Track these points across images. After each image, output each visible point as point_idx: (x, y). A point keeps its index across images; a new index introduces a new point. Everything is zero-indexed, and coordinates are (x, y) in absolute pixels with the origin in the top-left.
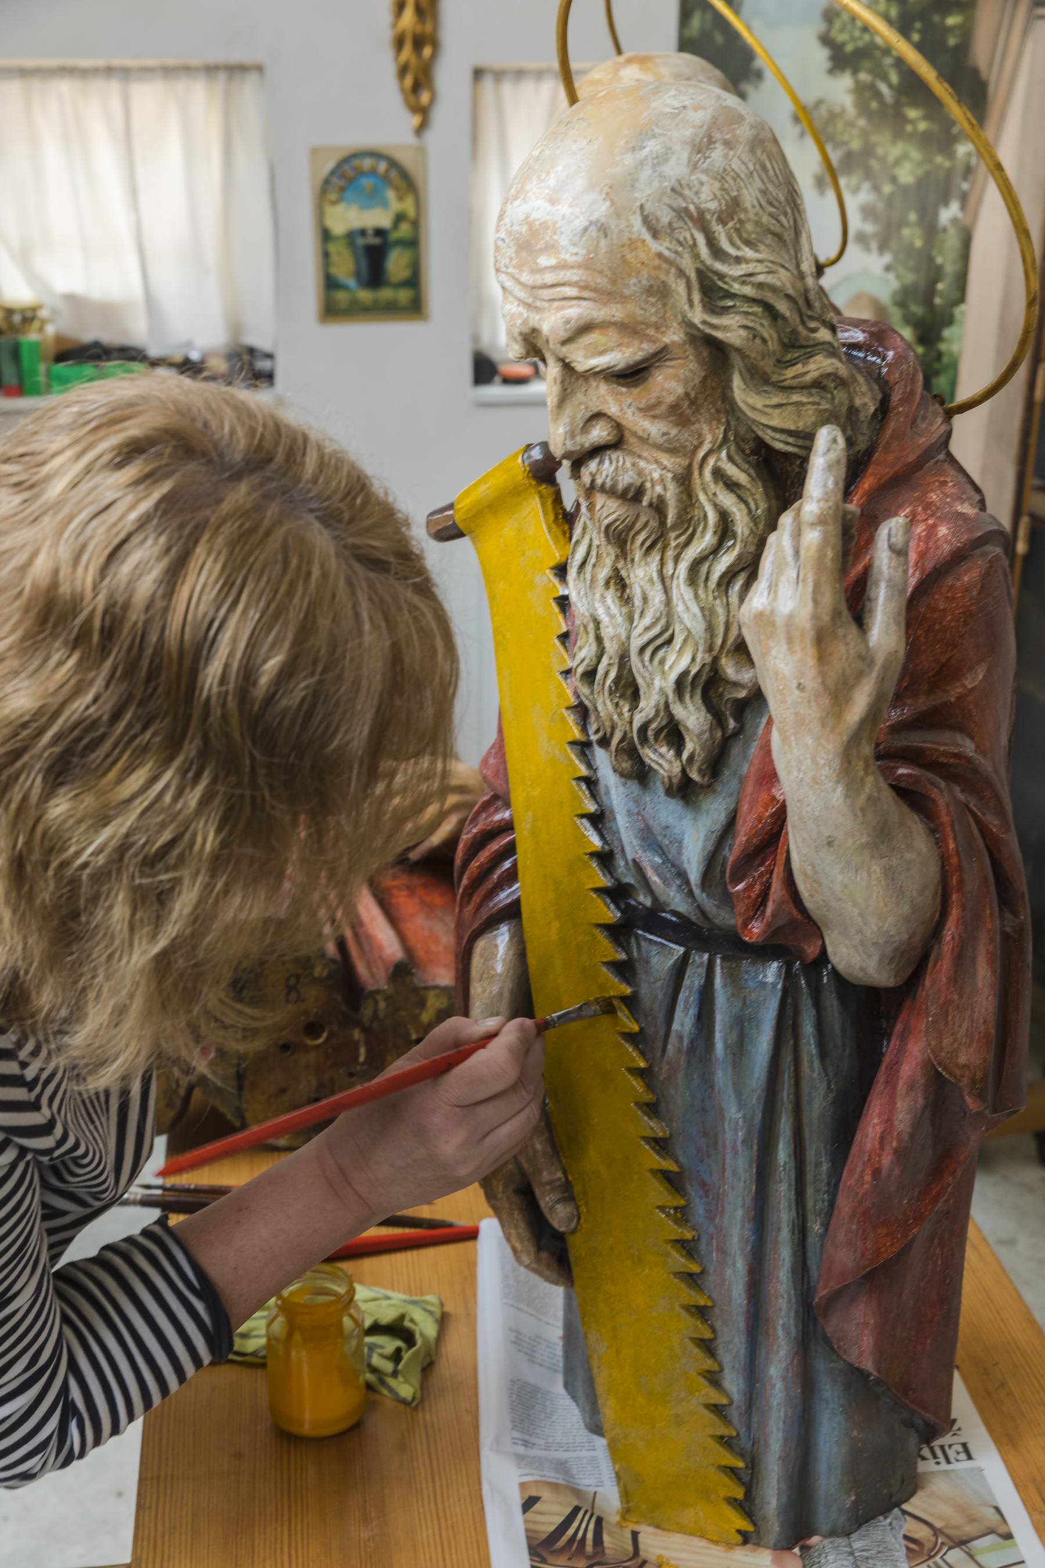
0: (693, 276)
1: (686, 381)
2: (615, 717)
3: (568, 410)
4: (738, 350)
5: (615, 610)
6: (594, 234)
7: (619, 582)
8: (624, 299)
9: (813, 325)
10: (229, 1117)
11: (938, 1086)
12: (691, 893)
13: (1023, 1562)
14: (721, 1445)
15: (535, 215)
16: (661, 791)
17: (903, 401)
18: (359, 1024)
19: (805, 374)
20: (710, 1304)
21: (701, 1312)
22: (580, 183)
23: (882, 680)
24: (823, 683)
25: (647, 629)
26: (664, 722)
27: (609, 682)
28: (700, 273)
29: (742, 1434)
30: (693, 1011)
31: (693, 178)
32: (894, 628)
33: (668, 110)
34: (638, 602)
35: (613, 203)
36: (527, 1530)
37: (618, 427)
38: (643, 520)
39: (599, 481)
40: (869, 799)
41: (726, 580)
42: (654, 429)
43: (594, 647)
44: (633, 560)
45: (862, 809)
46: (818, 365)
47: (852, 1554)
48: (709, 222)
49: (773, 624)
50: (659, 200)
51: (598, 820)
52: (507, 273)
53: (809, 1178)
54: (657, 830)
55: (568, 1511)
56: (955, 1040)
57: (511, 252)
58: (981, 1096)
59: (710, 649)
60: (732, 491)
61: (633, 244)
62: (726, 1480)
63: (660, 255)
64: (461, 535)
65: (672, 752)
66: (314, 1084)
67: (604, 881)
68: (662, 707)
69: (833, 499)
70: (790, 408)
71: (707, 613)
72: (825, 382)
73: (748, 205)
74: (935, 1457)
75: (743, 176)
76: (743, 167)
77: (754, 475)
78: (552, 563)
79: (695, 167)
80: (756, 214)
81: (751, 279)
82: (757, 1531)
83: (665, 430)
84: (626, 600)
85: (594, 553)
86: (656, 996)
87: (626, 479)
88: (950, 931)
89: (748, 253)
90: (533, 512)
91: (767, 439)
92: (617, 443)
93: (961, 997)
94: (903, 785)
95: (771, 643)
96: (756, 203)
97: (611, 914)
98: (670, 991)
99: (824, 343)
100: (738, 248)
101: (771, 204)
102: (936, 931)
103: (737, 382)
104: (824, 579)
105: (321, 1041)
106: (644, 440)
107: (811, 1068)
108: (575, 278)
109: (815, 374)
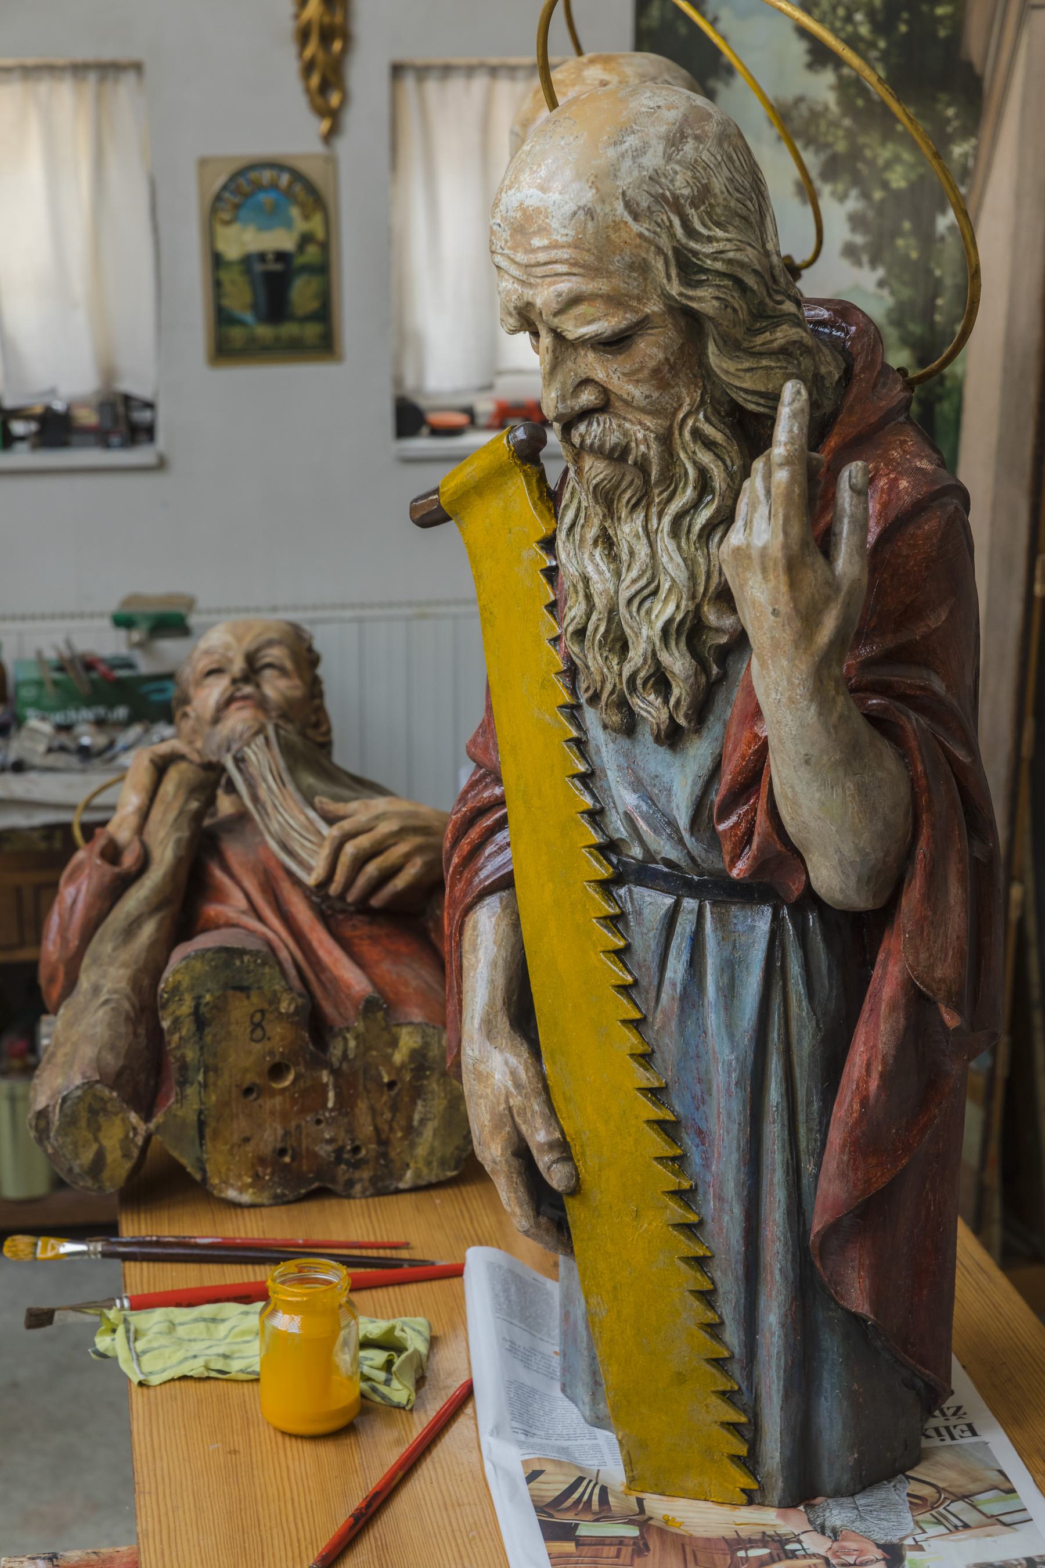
0: (670, 253)
1: (666, 348)
2: (605, 670)
3: (560, 377)
4: (710, 319)
5: (603, 567)
6: (582, 218)
7: (607, 541)
8: (609, 274)
9: (778, 298)
10: (189, 1169)
11: (917, 1001)
12: (681, 841)
13: (1025, 1510)
14: (724, 1401)
15: (528, 202)
16: (649, 739)
17: (863, 370)
18: (327, 1065)
19: (772, 341)
20: (709, 1254)
21: (700, 1263)
22: (568, 173)
23: (847, 605)
24: (796, 608)
25: (634, 581)
26: (652, 671)
27: (598, 637)
28: (676, 251)
29: (744, 1387)
30: (685, 957)
31: (668, 168)
32: (857, 558)
33: (644, 109)
34: (625, 556)
35: (598, 190)
36: (531, 1496)
37: (605, 392)
38: (628, 478)
39: (588, 442)
40: (840, 717)
41: (706, 532)
42: (636, 392)
43: (583, 605)
44: (619, 518)
45: (835, 727)
46: (784, 334)
47: (857, 1509)
48: (684, 206)
49: (749, 557)
50: (639, 188)
51: (587, 779)
52: (502, 254)
53: (802, 1117)
54: (647, 780)
55: (572, 1480)
56: (931, 955)
57: (506, 235)
58: (957, 1008)
59: (693, 597)
60: (710, 449)
61: (617, 226)
62: (729, 1436)
63: (641, 235)
64: (447, 519)
65: (659, 700)
66: (280, 1132)
67: (596, 838)
68: (649, 654)
69: (798, 442)
70: (760, 372)
71: (689, 563)
72: (791, 349)
73: (717, 191)
74: (939, 1434)
75: (712, 166)
76: (712, 159)
77: (730, 434)
78: (538, 537)
79: (669, 159)
80: (725, 199)
81: (722, 256)
82: (762, 1489)
83: (648, 393)
84: (613, 557)
85: (582, 515)
86: (650, 946)
87: (613, 439)
88: (922, 850)
89: (719, 233)
90: (518, 490)
91: (740, 401)
92: (605, 406)
93: (935, 913)
94: (874, 713)
95: (748, 575)
96: (724, 189)
98: (663, 940)
99: (790, 314)
100: (710, 229)
101: (738, 190)
102: (908, 855)
103: (711, 348)
104: (792, 513)
105: (287, 1083)
106: (627, 403)
107: (800, 1006)
108: (566, 256)
109: (781, 342)
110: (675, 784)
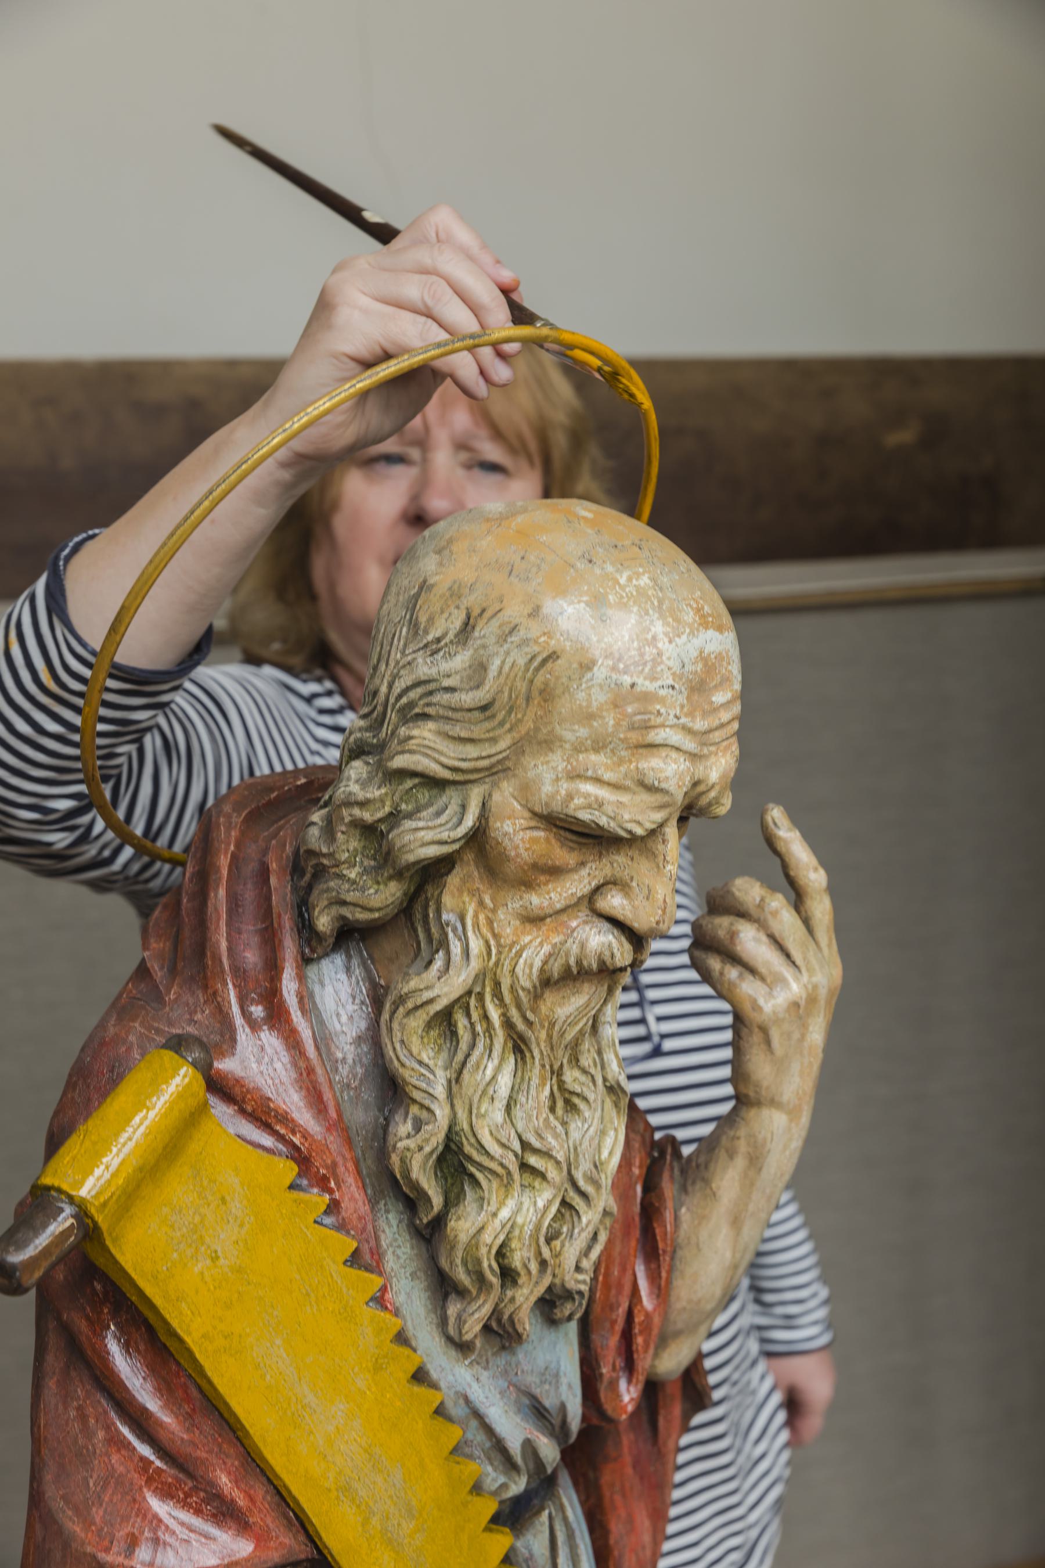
52: (671, 727)
57: (682, 699)
67: (490, 1507)
97: (502, 1541)
110: (562, 1364)
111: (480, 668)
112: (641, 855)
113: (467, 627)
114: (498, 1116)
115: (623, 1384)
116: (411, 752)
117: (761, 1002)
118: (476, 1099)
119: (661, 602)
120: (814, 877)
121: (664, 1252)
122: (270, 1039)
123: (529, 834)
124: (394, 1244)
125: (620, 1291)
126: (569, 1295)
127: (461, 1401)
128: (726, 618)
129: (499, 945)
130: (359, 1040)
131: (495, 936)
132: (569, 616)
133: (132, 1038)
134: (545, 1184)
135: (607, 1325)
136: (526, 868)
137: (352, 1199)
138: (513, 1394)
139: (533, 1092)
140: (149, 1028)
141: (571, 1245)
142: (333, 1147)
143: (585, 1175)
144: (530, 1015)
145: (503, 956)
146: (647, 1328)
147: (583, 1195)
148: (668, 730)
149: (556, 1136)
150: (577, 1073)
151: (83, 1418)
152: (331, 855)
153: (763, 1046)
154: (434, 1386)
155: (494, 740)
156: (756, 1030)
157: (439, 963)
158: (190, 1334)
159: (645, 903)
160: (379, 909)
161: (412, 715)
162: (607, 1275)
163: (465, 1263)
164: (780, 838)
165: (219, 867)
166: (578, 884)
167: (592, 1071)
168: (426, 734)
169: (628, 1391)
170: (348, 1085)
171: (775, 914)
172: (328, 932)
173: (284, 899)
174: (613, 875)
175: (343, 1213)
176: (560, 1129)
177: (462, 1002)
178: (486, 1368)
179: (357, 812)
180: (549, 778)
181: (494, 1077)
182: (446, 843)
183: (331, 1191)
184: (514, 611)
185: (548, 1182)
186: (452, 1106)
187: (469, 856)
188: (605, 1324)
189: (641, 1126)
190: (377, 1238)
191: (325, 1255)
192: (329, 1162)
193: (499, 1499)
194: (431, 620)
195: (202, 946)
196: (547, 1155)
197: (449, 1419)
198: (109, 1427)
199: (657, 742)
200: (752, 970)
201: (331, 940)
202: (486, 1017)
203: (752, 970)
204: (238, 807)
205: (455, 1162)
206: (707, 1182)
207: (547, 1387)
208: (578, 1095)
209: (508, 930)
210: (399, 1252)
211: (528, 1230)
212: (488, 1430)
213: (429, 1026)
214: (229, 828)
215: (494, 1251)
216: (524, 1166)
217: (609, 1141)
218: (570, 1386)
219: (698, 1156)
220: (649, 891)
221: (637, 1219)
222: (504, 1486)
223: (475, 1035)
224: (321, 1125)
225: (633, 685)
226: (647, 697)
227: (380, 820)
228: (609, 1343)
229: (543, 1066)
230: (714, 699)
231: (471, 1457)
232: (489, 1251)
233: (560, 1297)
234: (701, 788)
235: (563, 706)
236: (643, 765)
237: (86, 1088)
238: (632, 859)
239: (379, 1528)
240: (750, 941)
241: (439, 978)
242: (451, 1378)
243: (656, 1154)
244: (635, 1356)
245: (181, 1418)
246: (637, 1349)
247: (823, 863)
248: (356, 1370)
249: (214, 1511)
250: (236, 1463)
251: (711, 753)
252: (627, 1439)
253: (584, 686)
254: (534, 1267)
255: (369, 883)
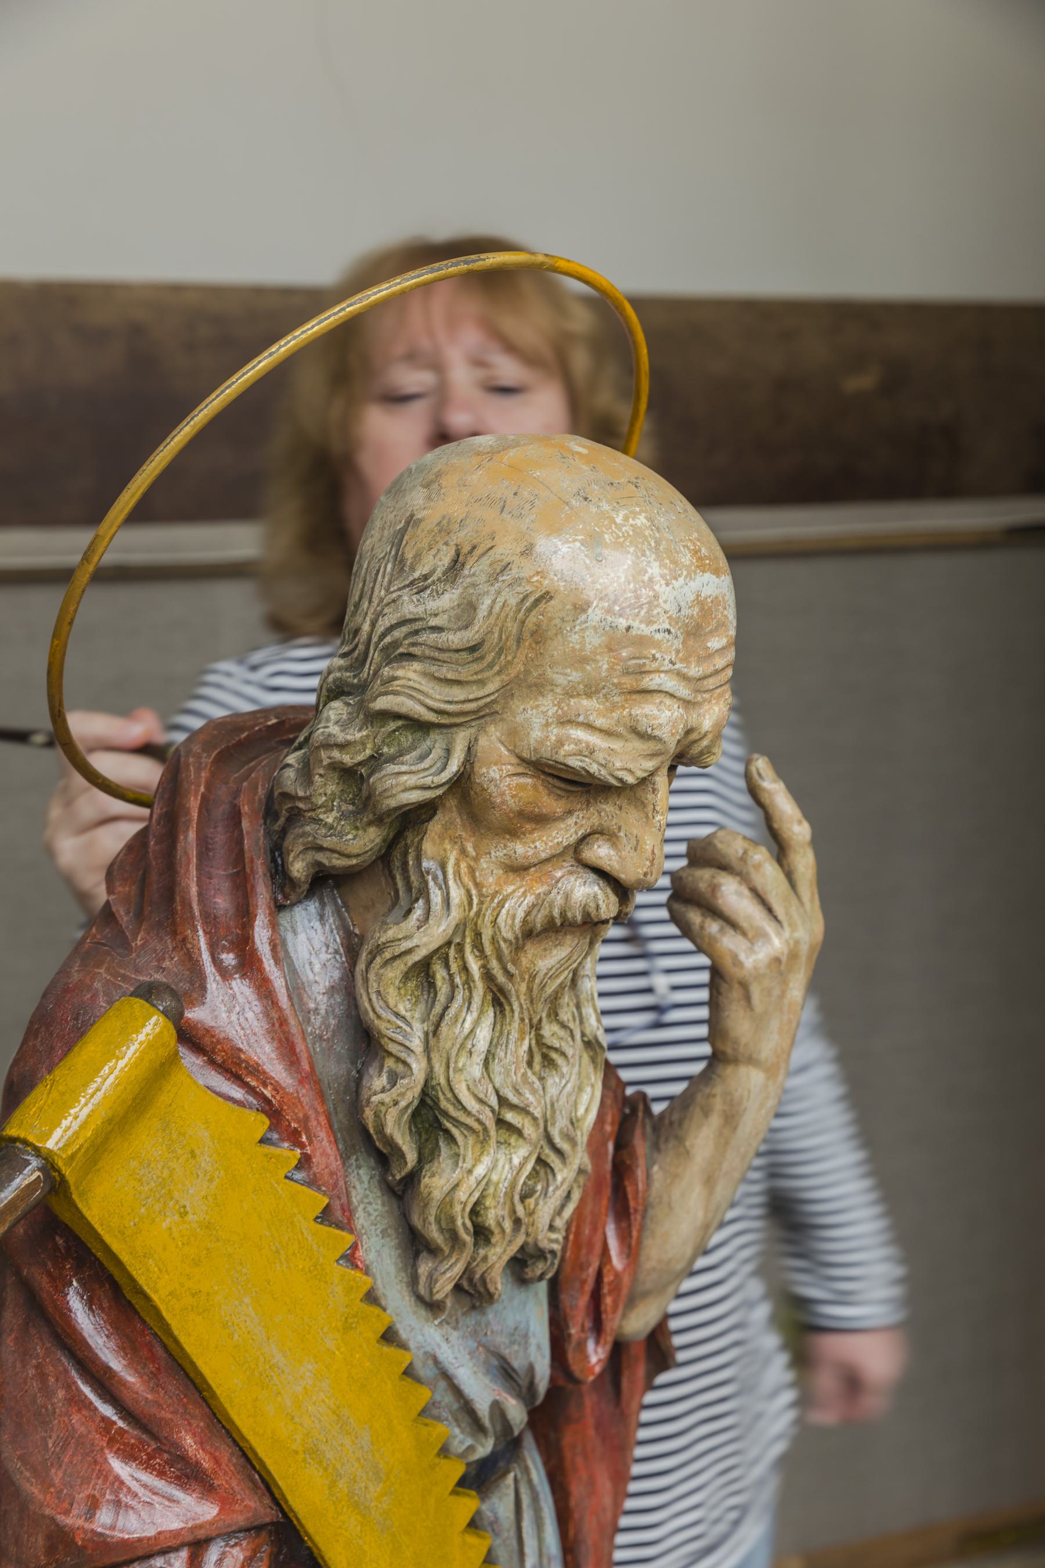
52: (666, 672)
57: (678, 644)
67: (458, 1470)
97: (468, 1505)
111: (469, 607)
112: (629, 804)
113: (456, 565)
114: (476, 1070)
115: (591, 1345)
116: (396, 693)
117: (742, 957)
118: (454, 1053)
119: (658, 543)
120: (798, 830)
121: (636, 1210)
122: (242, 988)
123: (516, 780)
124: (366, 1201)
125: (590, 1251)
126: (541, 1254)
127: (430, 1362)
128: (723, 562)
129: (481, 895)
130: (332, 990)
131: (477, 885)
132: (562, 557)
133: (97, 985)
134: (521, 1140)
135: (577, 1285)
136: (512, 815)
137: (324, 1154)
138: (482, 1354)
139: (512, 1046)
140: (116, 975)
141: (546, 1203)
142: (305, 1100)
143: (561, 1132)
144: (510, 967)
145: (485, 906)
146: (616, 1288)
147: (559, 1152)
148: (662, 675)
149: (534, 1092)
150: (555, 1028)
151: (42, 1376)
152: (307, 799)
153: (743, 1003)
154: (403, 1346)
155: (482, 683)
156: (736, 986)
157: (418, 912)
158: (156, 1292)
159: (633, 854)
160: (357, 856)
161: (397, 655)
162: (578, 1234)
163: (438, 1221)
164: (764, 789)
165: (189, 808)
166: (564, 834)
167: (571, 1025)
168: (411, 675)
169: (596, 1352)
170: (321, 1037)
171: (758, 867)
172: (303, 879)
173: (257, 844)
174: (600, 824)
175: (315, 1168)
176: (537, 1084)
177: (441, 953)
178: (455, 1328)
179: (336, 754)
180: (538, 723)
181: (472, 1031)
182: (429, 788)
183: (302, 1146)
184: (506, 549)
185: (525, 1139)
186: (429, 1059)
187: (452, 802)
188: (575, 1285)
189: (613, 1083)
190: (348, 1195)
191: (295, 1210)
192: (301, 1115)
193: (465, 1461)
194: (418, 556)
195: (171, 891)
196: (524, 1110)
197: (418, 1380)
198: (69, 1386)
199: (652, 688)
200: (733, 924)
201: (306, 887)
202: (465, 969)
203: (733, 924)
204: (208, 747)
205: (430, 1117)
206: (680, 1140)
207: (516, 1347)
208: (556, 1050)
209: (491, 880)
210: (370, 1209)
211: (503, 1187)
212: (457, 1391)
213: (406, 977)
214: (199, 770)
215: (468, 1209)
216: (501, 1122)
217: (585, 1097)
218: (539, 1347)
219: (671, 1113)
220: (638, 841)
221: (608, 1177)
222: (471, 1449)
223: (453, 987)
224: (293, 1078)
225: (628, 629)
226: (642, 641)
227: (360, 764)
228: (578, 1303)
229: (522, 1020)
230: (709, 645)
231: (438, 1419)
232: (463, 1209)
233: (532, 1257)
234: (694, 736)
235: (556, 649)
236: (637, 711)
237: (53, 1032)
238: (620, 808)
239: (346, 1490)
240: (731, 894)
241: (419, 928)
242: (420, 1338)
243: (627, 1111)
244: (604, 1316)
245: (145, 1377)
246: (606, 1311)
247: (807, 815)
248: (326, 1329)
249: (178, 1473)
250: (202, 1424)
251: (705, 700)
252: (590, 1401)
253: (578, 627)
254: (508, 1225)
255: (348, 828)
